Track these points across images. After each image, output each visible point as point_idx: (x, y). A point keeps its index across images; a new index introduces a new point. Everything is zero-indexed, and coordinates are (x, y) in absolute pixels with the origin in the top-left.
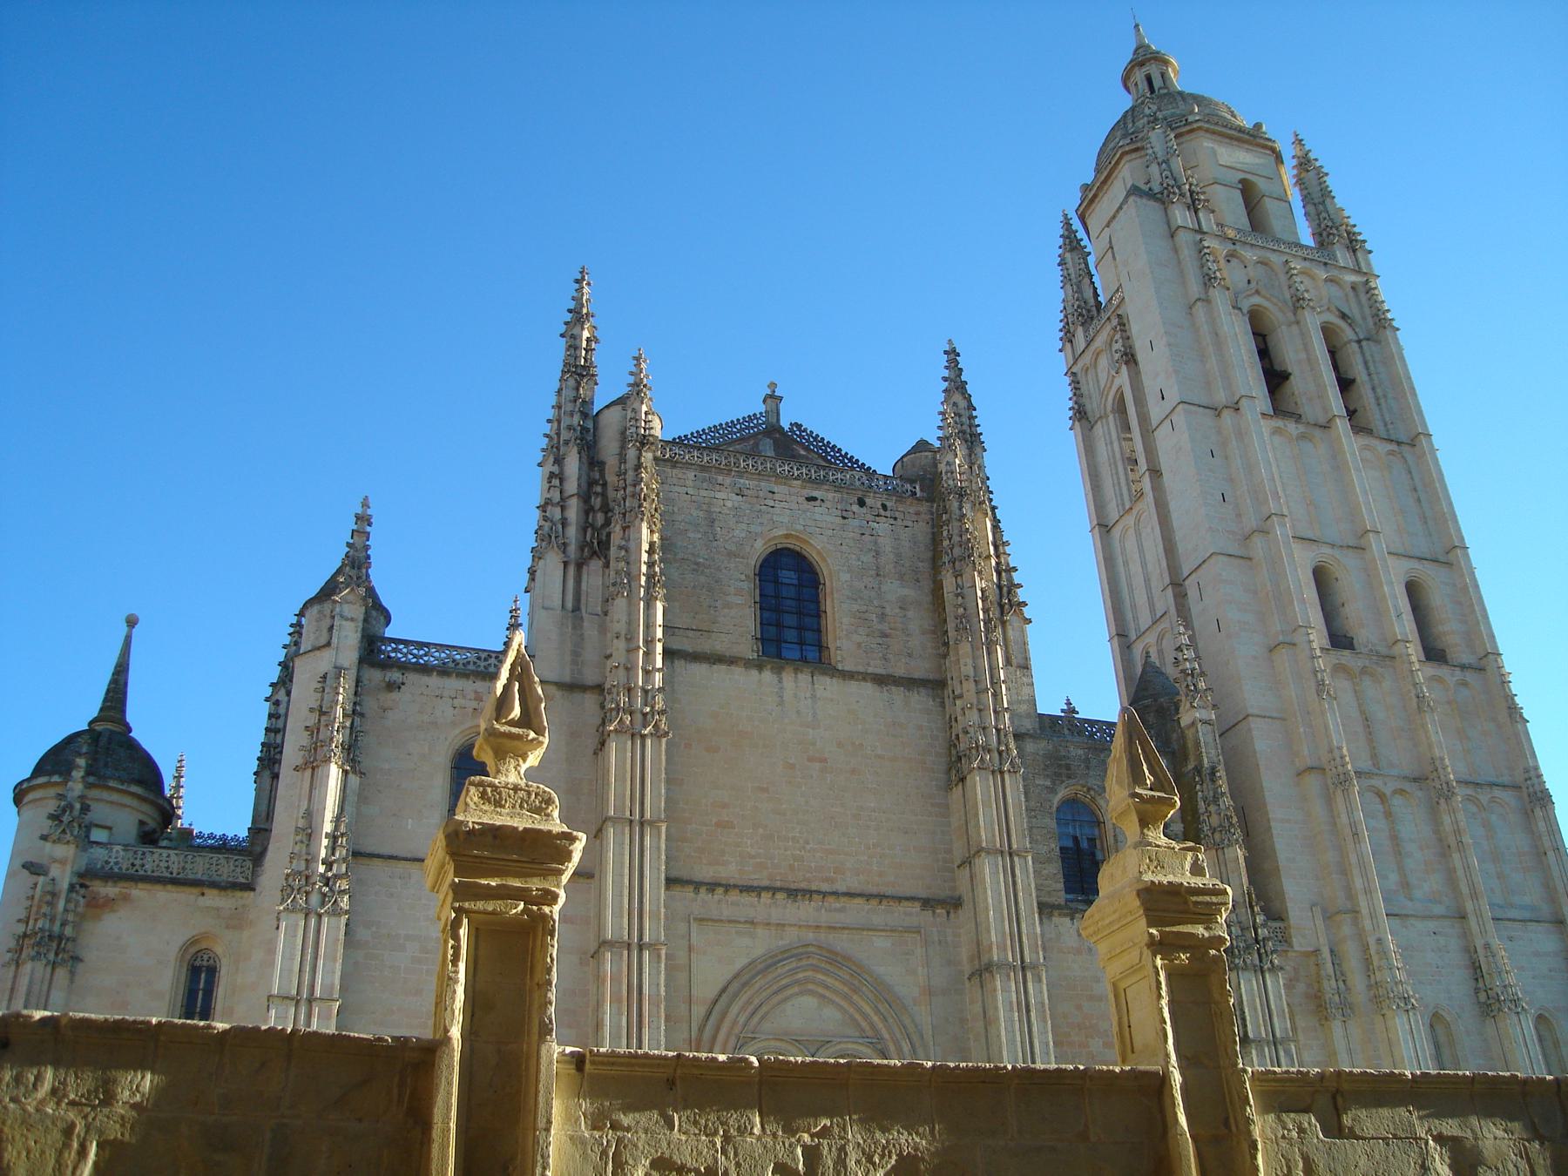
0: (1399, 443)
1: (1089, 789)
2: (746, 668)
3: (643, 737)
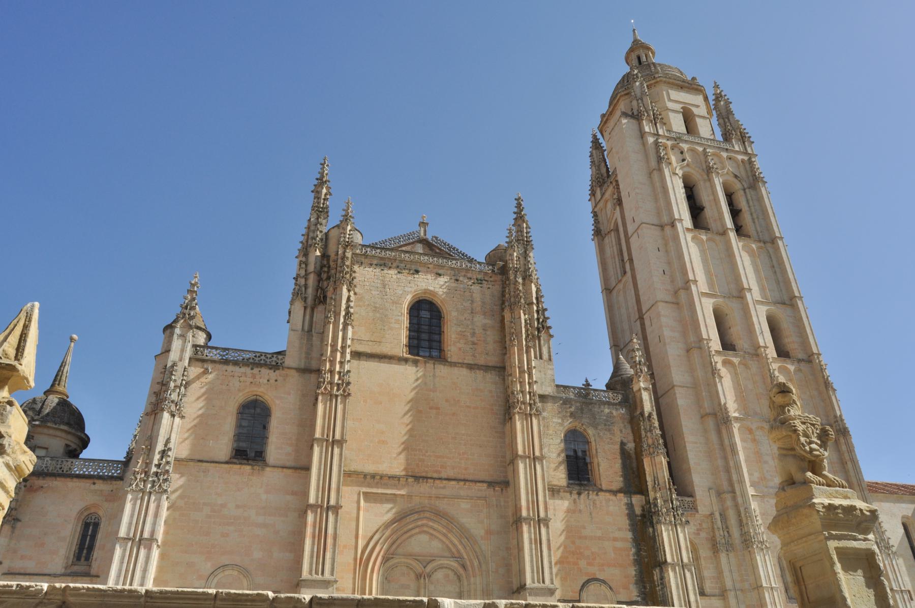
1: (582, 425)
3: (337, 396)
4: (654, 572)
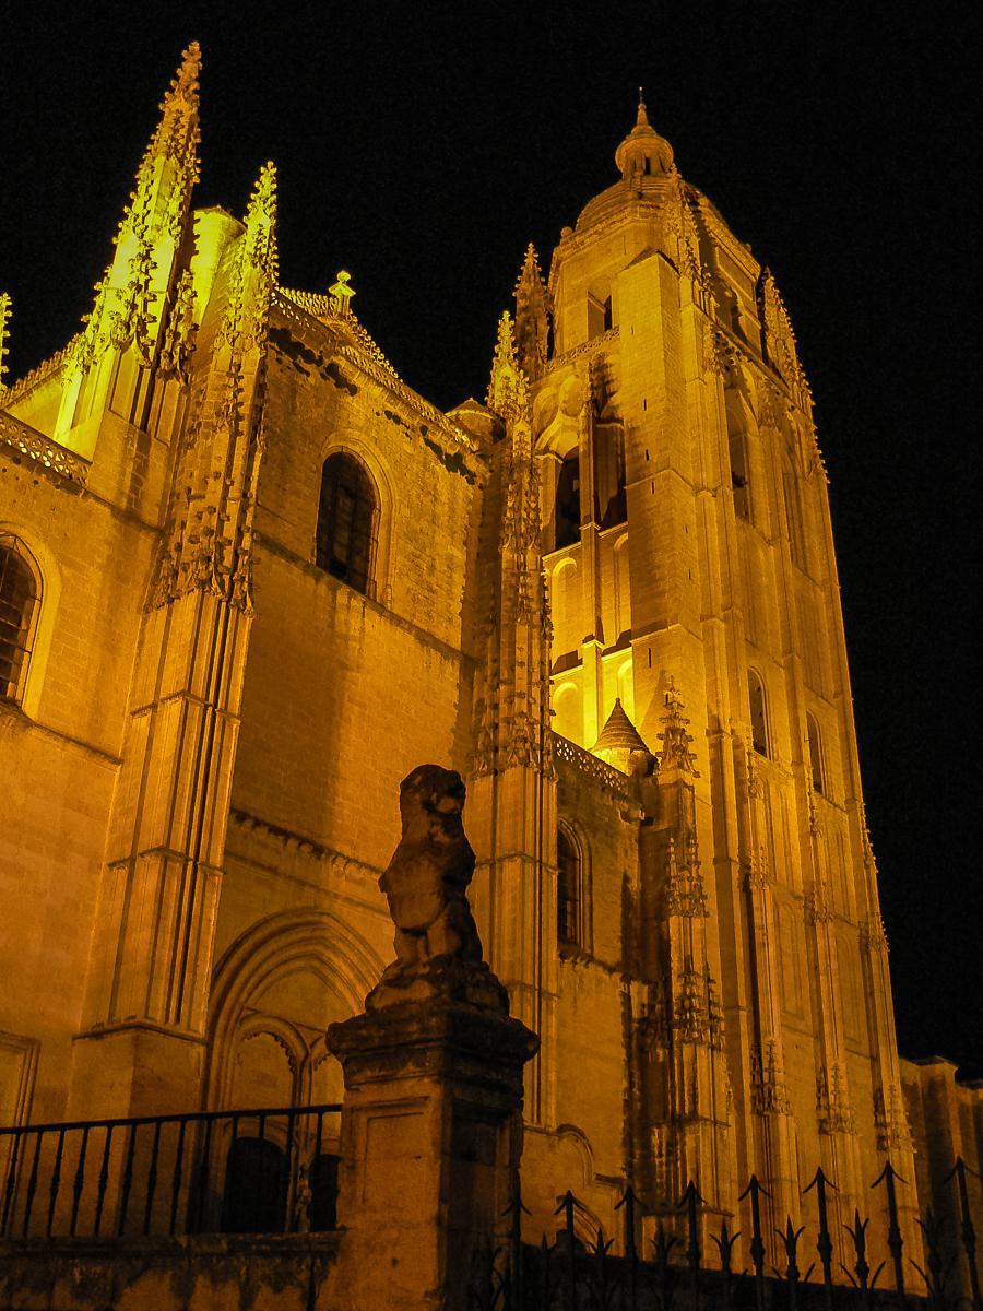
2: (305, 571)
4: (656, 1130)
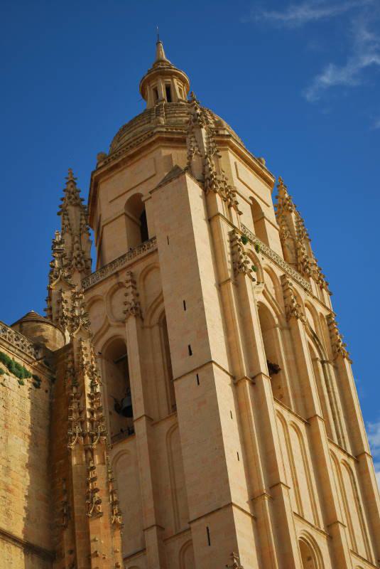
0: (349, 455)
